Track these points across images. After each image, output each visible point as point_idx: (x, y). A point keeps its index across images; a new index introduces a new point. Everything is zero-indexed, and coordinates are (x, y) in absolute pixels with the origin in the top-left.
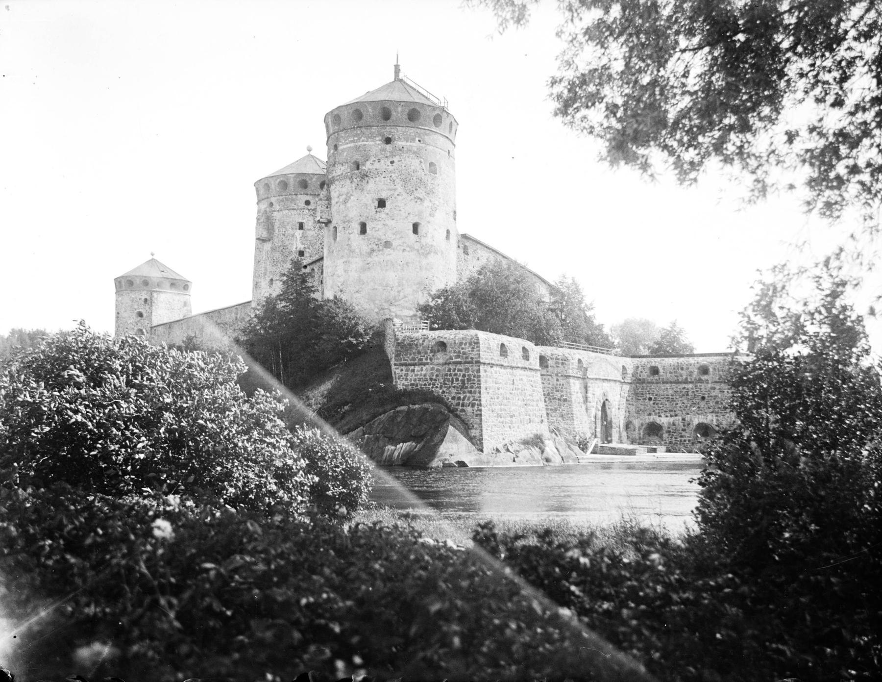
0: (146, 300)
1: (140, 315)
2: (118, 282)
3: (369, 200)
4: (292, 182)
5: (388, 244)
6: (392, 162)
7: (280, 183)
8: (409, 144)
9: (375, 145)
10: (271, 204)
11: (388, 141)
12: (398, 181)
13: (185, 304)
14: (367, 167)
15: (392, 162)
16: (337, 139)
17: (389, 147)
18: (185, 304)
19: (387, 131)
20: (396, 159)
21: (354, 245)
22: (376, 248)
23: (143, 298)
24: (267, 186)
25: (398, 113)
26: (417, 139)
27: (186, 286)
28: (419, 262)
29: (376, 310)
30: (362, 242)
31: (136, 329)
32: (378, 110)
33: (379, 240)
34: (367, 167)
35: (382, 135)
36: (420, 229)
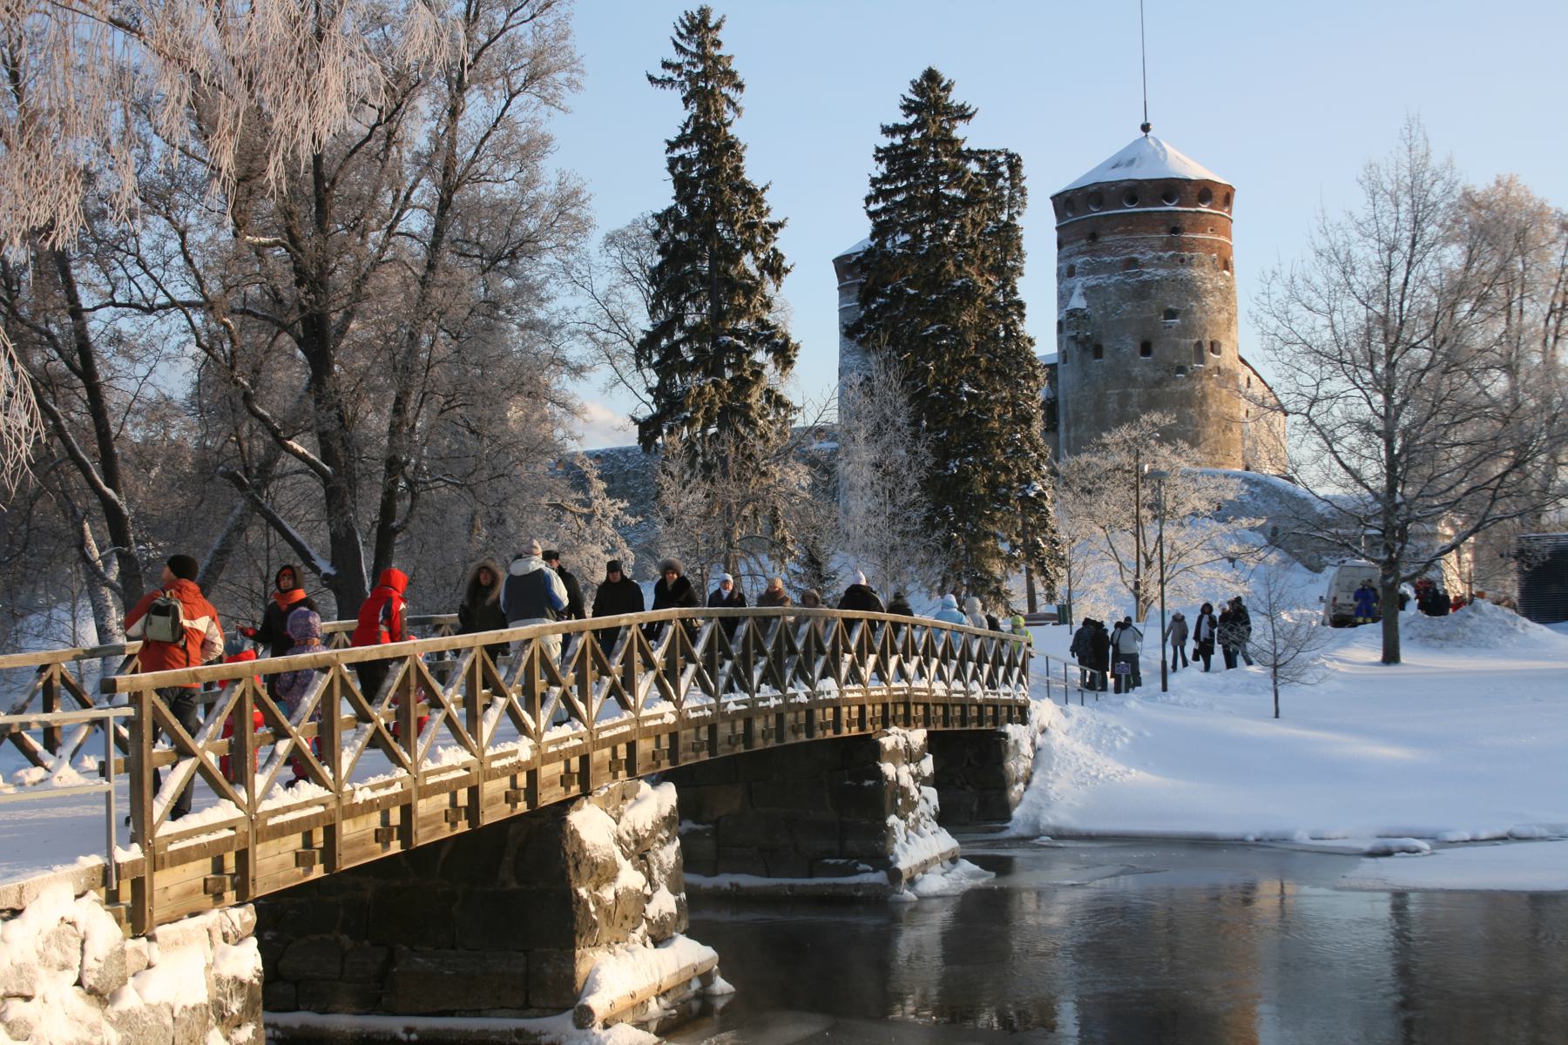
21: (1136, 371)
33: (1171, 364)
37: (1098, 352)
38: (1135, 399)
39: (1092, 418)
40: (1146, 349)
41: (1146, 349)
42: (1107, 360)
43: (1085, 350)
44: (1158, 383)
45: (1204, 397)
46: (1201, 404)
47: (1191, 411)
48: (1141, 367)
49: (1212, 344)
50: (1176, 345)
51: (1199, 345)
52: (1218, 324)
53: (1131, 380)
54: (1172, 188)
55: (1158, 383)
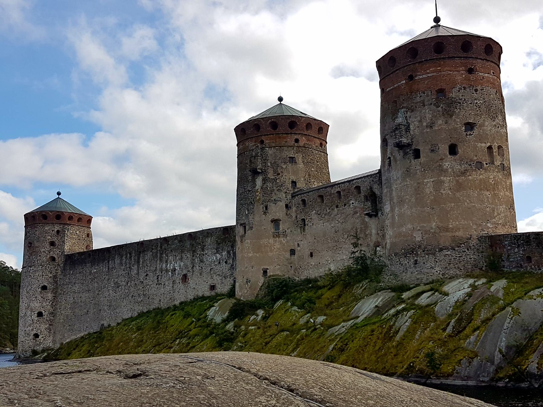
0: (58, 232)
3: (457, 123)
5: (479, 165)
6: (476, 90)
7: (273, 122)
8: (486, 75)
9: (460, 75)
10: (262, 142)
11: (470, 71)
12: (483, 107)
13: (88, 235)
14: (453, 94)
15: (476, 90)
17: (471, 77)
20: (479, 88)
21: (446, 165)
23: (56, 230)
26: (492, 71)
27: (89, 220)
29: (475, 227)
30: (454, 163)
31: (48, 256)
33: (471, 160)
35: (466, 66)
37: (417, 154)
39: (413, 200)
40: (453, 150)
41: (453, 150)
42: (422, 159)
43: (405, 154)
44: (464, 173)
45: (496, 184)
46: (494, 189)
47: (488, 193)
48: (449, 163)
49: (500, 147)
51: (490, 148)
53: (443, 171)
55: (464, 173)
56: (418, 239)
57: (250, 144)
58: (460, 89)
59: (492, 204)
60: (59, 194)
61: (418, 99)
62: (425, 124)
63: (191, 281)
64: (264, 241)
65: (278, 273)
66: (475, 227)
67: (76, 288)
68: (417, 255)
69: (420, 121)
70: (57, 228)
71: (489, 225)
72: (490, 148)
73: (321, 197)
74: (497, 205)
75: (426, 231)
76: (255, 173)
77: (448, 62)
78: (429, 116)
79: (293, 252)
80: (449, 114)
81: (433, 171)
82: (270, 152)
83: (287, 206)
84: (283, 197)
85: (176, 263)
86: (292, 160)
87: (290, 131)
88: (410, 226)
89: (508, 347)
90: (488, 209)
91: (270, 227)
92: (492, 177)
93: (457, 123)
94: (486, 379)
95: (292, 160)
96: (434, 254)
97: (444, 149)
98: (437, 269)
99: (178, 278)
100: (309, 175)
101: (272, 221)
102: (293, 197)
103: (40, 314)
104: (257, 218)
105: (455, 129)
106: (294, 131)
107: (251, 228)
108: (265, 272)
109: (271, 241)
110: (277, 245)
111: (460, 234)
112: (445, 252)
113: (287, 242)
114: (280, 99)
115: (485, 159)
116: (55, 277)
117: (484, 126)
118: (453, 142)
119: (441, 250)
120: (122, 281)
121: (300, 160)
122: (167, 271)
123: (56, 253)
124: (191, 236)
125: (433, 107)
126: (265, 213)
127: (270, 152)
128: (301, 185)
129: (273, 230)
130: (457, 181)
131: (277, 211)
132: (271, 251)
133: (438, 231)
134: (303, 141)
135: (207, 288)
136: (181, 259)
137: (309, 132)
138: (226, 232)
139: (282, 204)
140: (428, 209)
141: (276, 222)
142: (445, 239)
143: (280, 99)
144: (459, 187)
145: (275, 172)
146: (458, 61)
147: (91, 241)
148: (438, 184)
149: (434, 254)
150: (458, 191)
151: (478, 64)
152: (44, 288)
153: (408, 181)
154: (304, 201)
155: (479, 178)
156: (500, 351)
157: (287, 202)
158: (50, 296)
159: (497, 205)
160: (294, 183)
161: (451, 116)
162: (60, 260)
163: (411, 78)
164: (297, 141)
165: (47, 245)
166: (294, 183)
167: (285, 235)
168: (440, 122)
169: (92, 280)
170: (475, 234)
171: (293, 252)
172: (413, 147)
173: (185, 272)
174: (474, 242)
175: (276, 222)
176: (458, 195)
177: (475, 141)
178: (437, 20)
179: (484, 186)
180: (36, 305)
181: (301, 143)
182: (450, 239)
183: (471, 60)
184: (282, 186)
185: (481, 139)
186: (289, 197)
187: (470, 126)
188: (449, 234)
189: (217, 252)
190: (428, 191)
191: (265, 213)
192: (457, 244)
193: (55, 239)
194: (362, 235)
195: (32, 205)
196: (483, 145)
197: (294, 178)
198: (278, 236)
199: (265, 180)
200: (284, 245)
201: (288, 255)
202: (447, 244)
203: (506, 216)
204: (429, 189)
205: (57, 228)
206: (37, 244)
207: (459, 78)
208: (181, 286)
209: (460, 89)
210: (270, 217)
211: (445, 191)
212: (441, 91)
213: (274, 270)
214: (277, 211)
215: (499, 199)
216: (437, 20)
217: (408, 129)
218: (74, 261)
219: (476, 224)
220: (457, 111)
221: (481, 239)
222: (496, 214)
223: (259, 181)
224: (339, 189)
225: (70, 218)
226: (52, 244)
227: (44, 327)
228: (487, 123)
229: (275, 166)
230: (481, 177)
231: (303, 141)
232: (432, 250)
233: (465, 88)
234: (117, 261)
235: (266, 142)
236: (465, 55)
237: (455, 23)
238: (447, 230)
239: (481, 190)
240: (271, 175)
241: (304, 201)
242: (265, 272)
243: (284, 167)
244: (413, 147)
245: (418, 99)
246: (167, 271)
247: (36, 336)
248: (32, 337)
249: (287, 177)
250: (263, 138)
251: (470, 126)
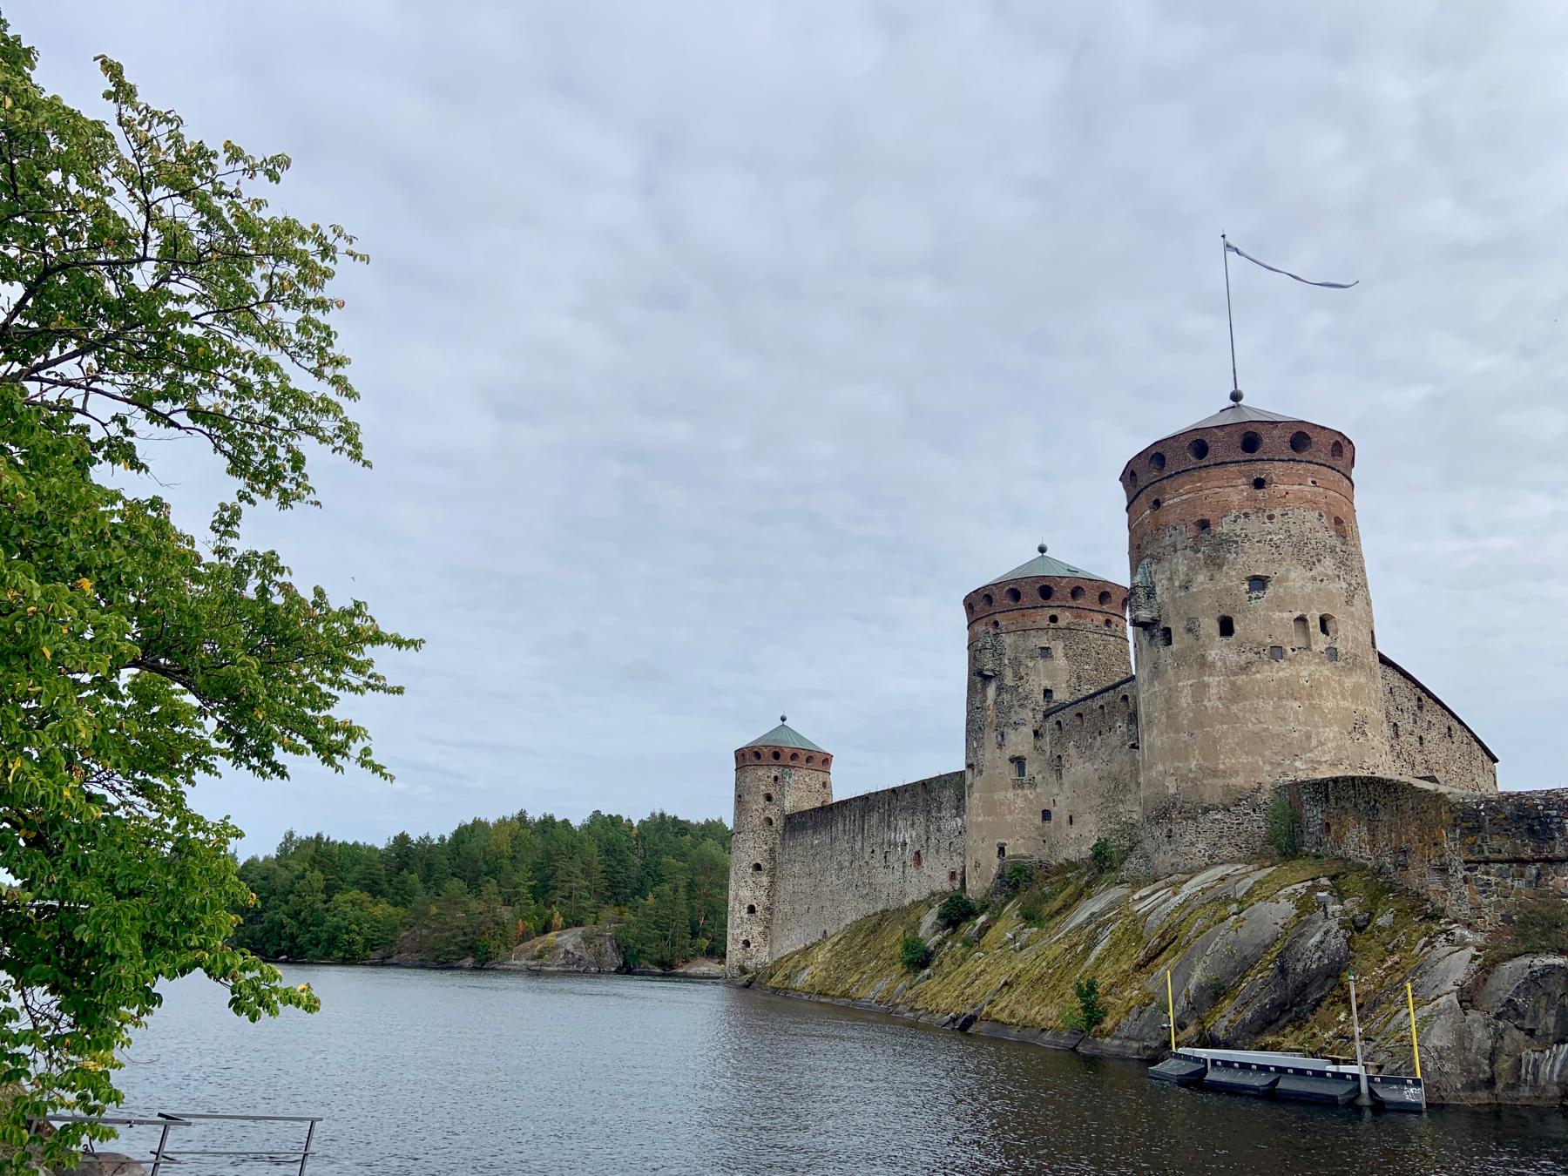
0: (776, 778)
1: (769, 798)
2: (741, 755)
4: (1025, 590)
5: (1277, 652)
6: (1271, 517)
9: (1236, 492)
10: (996, 624)
11: (1259, 484)
12: (1285, 547)
13: (824, 785)
14: (1224, 528)
15: (1271, 517)
16: (1162, 491)
17: (1260, 493)
18: (824, 785)
19: (1258, 469)
20: (1277, 512)
21: (1212, 655)
22: (1256, 658)
24: (989, 599)
25: (1274, 442)
27: (827, 760)
28: (1340, 683)
30: (1226, 650)
32: (1237, 440)
33: (1260, 644)
34: (1224, 528)
36: (1330, 625)
38: (1214, 691)
39: (1164, 719)
40: (1226, 627)
41: (1226, 627)
42: (1175, 646)
43: (1152, 637)
44: (1245, 668)
45: (1315, 688)
46: (1310, 696)
47: (1296, 704)
48: (1218, 650)
50: (1268, 621)
51: (1302, 620)
52: (1331, 596)
53: (1204, 664)
54: (1250, 438)
55: (1245, 668)
56: (1172, 791)
57: (980, 628)
58: (1237, 517)
59: (1305, 724)
60: (783, 719)
61: (1167, 540)
62: (1177, 584)
63: (924, 863)
64: (999, 795)
65: (1023, 851)
66: (1268, 768)
67: (797, 868)
68: (1171, 819)
69: (1170, 579)
70: (774, 772)
71: (1298, 764)
72: (1302, 620)
73: (1080, 715)
74: (1316, 727)
75: (1182, 776)
76: (987, 679)
77: (1214, 471)
78: (1182, 569)
79: (1046, 815)
80: (1215, 564)
81: (1191, 666)
82: (1008, 640)
83: (1036, 733)
84: (1029, 717)
85: (906, 833)
86: (1046, 652)
87: (1041, 601)
88: (1160, 768)
89: (1201, 989)
90: (1296, 735)
91: (1010, 772)
92: (1305, 673)
93: (1233, 578)
94: (1155, 1044)
95: (1046, 652)
96: (1195, 819)
97: (1210, 626)
98: (1200, 846)
99: (909, 856)
100: (1079, 678)
101: (1012, 760)
102: (1046, 716)
103: (752, 910)
104: (988, 756)
105: (1228, 590)
106: (1049, 602)
107: (981, 772)
108: (1002, 850)
109: (1010, 795)
110: (1020, 803)
111: (1238, 781)
112: (1213, 815)
113: (1037, 797)
114: (1042, 550)
115: (1290, 639)
116: (772, 850)
117: (1287, 579)
118: (1223, 612)
119: (1206, 811)
120: (846, 859)
121: (1058, 649)
122: (896, 845)
123: (773, 812)
124: (924, 784)
125: (1188, 552)
126: (1000, 746)
127: (1008, 640)
128: (1061, 695)
129: (1015, 776)
130: (1233, 684)
131: (1020, 741)
132: (1011, 813)
133: (1200, 775)
134: (1065, 618)
135: (946, 877)
136: (913, 825)
137: (1080, 602)
138: (955, 782)
139: (1028, 731)
140: (1185, 736)
141: (1019, 762)
142: (1212, 792)
143: (1042, 550)
144: (1237, 694)
145: (1016, 674)
146: (1233, 468)
147: (830, 794)
148: (1200, 689)
149: (1195, 819)
150: (1234, 701)
151: (1276, 470)
152: (758, 867)
153: (1157, 687)
154: (1059, 723)
155: (1276, 676)
156: (1187, 996)
157: (1037, 726)
158: (765, 880)
159: (1316, 727)
160: (1048, 693)
161: (1220, 566)
162: (778, 824)
163: (1157, 504)
164: (1054, 619)
165: (762, 800)
166: (1048, 693)
167: (1033, 784)
168: (1201, 578)
169: (814, 856)
170: (1268, 782)
171: (1046, 815)
172: (1162, 625)
173: (917, 848)
174: (1264, 797)
175: (1019, 762)
176: (1234, 708)
177: (1268, 609)
178: (1236, 397)
179: (1288, 690)
180: (746, 894)
181: (1061, 623)
182: (1220, 791)
183: (1259, 465)
184: (1026, 698)
185: (1280, 605)
186: (1040, 716)
187: (1259, 583)
188: (1220, 782)
189: (958, 815)
190: (1184, 702)
191: (1000, 746)
192: (1235, 801)
193: (771, 791)
194: (1133, 785)
195: (745, 739)
196: (1286, 615)
197: (1047, 684)
198: (1021, 786)
199: (1000, 689)
200: (1031, 802)
201: (1038, 820)
202: (1216, 801)
203: (1339, 748)
204: (1185, 700)
205: (774, 772)
206: (747, 798)
207: (1235, 498)
208: (911, 871)
209: (1237, 517)
210: (1009, 752)
211: (1212, 702)
212: (1204, 525)
213: (1018, 847)
214: (1020, 741)
215: (1323, 716)
216: (1236, 397)
217: (1151, 594)
218: (796, 823)
219: (1271, 763)
220: (1231, 557)
221: (1279, 790)
222: (1314, 743)
223: (991, 691)
224: (1101, 703)
225: (794, 756)
226: (769, 798)
227: (757, 929)
228: (1293, 575)
229: (1016, 663)
230: (1281, 674)
231: (1065, 618)
232: (1195, 811)
233: (1246, 515)
234: (841, 827)
235: (1002, 623)
236: (1248, 456)
237: (1272, 399)
238: (1215, 773)
239: (1280, 698)
240: (1009, 680)
241: (1059, 723)
242: (1002, 850)
243: (1031, 665)
244: (1162, 625)
245: (1167, 540)
246: (896, 845)
247: (747, 944)
248: (740, 945)
249: (1036, 683)
250: (997, 617)
251: (1259, 583)
